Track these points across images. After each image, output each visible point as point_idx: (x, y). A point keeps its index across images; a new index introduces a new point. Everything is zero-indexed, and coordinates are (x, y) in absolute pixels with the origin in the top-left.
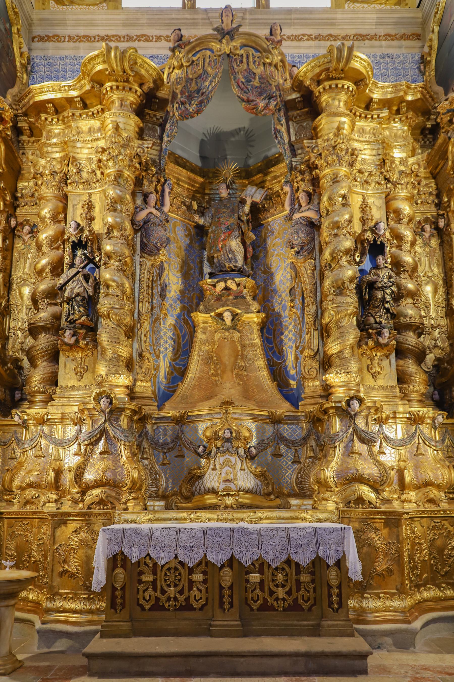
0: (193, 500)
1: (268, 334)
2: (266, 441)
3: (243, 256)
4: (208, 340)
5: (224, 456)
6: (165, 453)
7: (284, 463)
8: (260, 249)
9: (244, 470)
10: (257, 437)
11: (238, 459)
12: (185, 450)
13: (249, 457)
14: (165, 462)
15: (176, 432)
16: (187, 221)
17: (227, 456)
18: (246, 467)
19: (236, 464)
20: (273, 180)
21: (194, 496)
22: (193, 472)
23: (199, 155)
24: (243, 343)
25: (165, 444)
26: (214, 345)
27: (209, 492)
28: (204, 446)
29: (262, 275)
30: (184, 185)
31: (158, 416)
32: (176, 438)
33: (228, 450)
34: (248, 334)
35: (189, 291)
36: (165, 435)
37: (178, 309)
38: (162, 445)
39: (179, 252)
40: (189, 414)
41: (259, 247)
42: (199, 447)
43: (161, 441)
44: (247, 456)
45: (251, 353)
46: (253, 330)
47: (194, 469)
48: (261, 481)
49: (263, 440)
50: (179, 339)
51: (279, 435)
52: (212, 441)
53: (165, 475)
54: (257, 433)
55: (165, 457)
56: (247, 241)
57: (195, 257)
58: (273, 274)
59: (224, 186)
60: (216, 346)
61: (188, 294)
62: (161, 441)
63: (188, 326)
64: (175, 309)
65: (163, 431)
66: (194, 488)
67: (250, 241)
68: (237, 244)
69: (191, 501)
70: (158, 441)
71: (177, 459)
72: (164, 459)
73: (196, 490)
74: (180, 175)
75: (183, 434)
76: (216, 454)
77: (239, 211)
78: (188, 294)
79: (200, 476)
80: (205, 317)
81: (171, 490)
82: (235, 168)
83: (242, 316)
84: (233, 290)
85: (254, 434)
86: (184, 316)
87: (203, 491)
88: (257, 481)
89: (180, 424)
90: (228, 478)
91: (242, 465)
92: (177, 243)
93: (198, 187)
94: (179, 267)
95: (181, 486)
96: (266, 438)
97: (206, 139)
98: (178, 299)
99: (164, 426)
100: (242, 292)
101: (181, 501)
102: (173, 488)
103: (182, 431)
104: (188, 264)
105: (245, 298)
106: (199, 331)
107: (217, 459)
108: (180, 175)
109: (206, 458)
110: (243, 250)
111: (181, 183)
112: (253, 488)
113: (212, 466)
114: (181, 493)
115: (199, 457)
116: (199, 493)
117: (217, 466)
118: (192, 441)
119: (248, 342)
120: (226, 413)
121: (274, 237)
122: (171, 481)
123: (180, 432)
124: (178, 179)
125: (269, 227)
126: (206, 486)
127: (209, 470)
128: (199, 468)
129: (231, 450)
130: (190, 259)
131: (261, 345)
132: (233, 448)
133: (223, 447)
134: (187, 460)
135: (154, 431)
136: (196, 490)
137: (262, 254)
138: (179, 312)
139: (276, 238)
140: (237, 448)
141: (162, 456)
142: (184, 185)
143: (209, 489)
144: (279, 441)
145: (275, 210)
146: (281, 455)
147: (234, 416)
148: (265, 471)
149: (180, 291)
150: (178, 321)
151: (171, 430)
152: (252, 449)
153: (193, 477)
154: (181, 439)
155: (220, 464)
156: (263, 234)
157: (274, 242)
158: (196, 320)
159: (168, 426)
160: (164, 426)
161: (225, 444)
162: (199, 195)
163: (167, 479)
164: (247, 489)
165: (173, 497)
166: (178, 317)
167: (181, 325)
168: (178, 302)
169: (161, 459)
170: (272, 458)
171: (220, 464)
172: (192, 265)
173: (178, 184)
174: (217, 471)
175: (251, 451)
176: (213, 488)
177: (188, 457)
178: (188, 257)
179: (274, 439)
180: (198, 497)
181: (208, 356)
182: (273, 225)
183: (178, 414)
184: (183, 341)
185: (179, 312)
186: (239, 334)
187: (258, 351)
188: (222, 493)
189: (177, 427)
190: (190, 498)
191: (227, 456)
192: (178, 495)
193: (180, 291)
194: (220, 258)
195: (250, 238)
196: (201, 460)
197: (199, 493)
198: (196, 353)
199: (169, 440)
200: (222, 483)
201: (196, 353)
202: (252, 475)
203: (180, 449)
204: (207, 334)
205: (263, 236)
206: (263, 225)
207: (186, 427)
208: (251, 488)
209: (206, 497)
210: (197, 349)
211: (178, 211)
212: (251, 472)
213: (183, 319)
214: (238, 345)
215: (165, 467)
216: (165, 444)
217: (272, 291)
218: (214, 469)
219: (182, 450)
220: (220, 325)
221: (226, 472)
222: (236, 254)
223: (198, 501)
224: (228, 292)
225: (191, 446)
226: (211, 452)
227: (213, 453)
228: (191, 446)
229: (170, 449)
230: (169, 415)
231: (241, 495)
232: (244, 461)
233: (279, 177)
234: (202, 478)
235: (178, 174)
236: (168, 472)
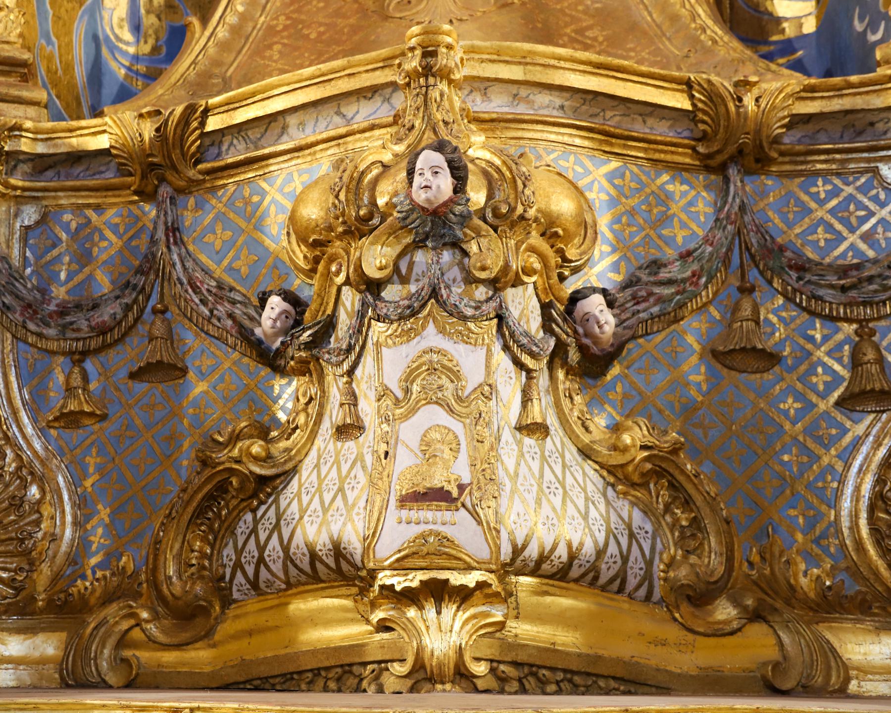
0: (226, 628)
2: (674, 271)
5: (408, 335)
6: (79, 357)
7: (791, 405)
9: (539, 430)
10: (620, 245)
11: (502, 360)
12: (190, 338)
13: (574, 356)
14: (72, 406)
15: (143, 243)
17: (431, 337)
18: (552, 421)
19: (488, 391)
21: (227, 601)
22: (222, 455)
25: (78, 307)
27: (315, 578)
28: (290, 297)
31: (40, 149)
32: (140, 271)
33: (434, 293)
36: (84, 258)
38: (63, 311)
40: (213, 123)
42: (263, 300)
43: (60, 293)
44: (560, 350)
47: (235, 438)
48: (647, 512)
49: (656, 265)
51: (754, 240)
52: (337, 247)
53: (75, 483)
54: (617, 220)
55: (76, 380)
62: (60, 293)
65: (74, 236)
66: (229, 551)
69: (209, 634)
70: (44, 291)
71: (140, 387)
72: (70, 390)
73: (238, 566)
75: (180, 243)
76: (360, 329)
79: (263, 480)
81: (100, 566)
85: (604, 223)
87: (277, 568)
88: (624, 507)
89: (165, 191)
90: (438, 481)
91: (526, 399)
95: (158, 542)
96: (670, 253)
99: (79, 209)
101: (151, 627)
102: (111, 556)
103: (174, 231)
107: (367, 364)
109: (303, 370)
112: (600, 553)
113: (335, 414)
114: (155, 584)
115: (265, 371)
116: (254, 584)
117: (367, 408)
118: (229, 280)
120: (427, 71)
122: (104, 512)
123: (160, 234)
126: (298, 539)
127: (319, 442)
128: (263, 433)
129: (456, 293)
132: (470, 280)
133: (404, 280)
134: (199, 388)
135: (24, 240)
136: (238, 566)
140: (496, 284)
141: (60, 378)
143: (314, 556)
144: (753, 275)
146: (770, 359)
147: (480, 105)
148: (675, 450)
151: (114, 228)
152: (595, 304)
153: (222, 488)
154: (166, 278)
155: (384, 393)
159: (98, 208)
160: (79, 209)
161: (420, 257)
163: (82, 503)
164: (562, 552)
165: (114, 607)
169: (55, 395)
170: (711, 375)
171: (384, 393)
174: (367, 438)
175: (586, 318)
176: (338, 551)
177: (202, 376)
179: (726, 261)
180: (253, 605)
183: (148, 130)
188: (399, 582)
189: (150, 210)
190: (205, 611)
191: (431, 337)
192: (137, 596)
196: (278, 383)
197: (254, 584)
199: (104, 283)
200: (393, 513)
202: (589, 467)
203: (159, 329)
207: (198, 207)
208: (589, 549)
209: (300, 606)
212: (586, 453)
215: (75, 436)
216: (78, 307)
218: (343, 431)
219: (170, 336)
221: (426, 444)
223: (250, 633)
225: (222, 310)
226: (330, 324)
227: (344, 321)
228: (222, 310)
229: (102, 330)
230: (102, 142)
231: (523, 596)
232: (543, 380)
234: (276, 492)
236: (92, 461)
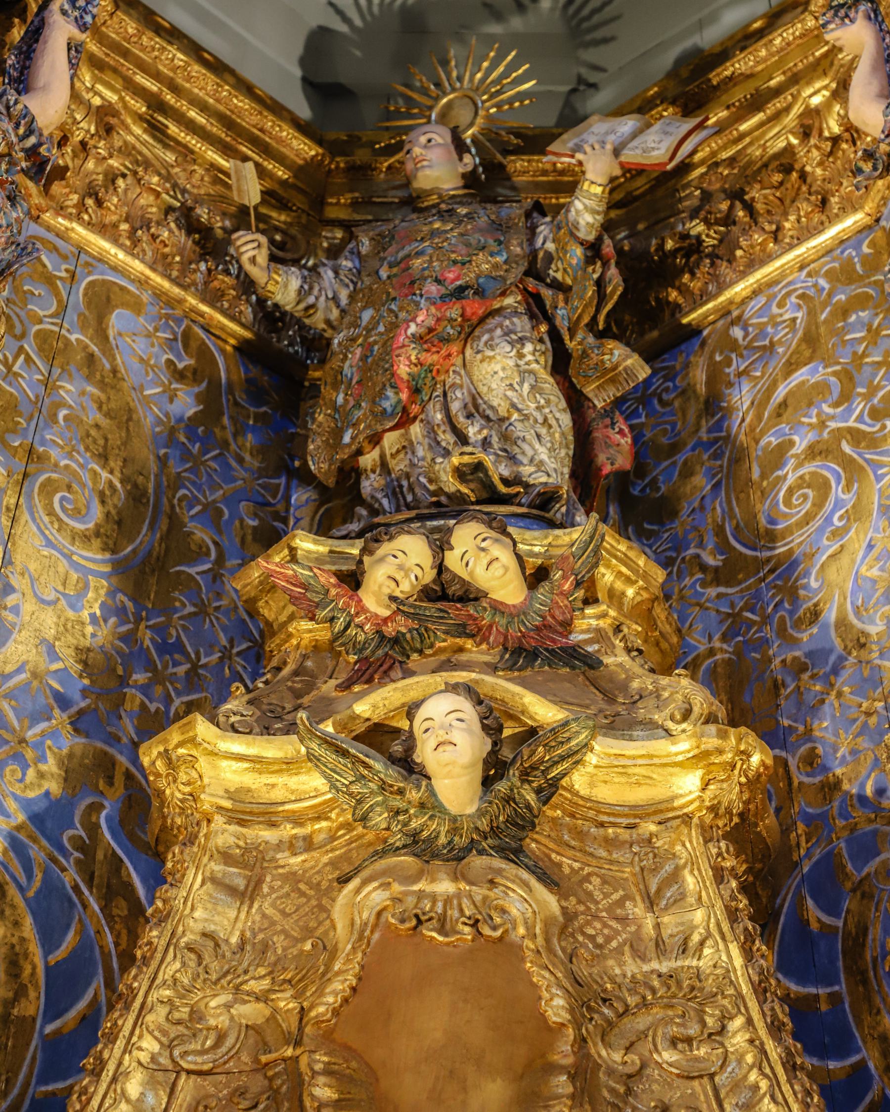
1: (801, 980)
3: (566, 453)
4: (265, 947)
8: (680, 458)
16: (192, 301)
20: (740, 117)
23: (297, 73)
24: (584, 971)
26: (325, 978)
29: (712, 592)
30: (192, 141)
34: (637, 909)
35: (158, 677)
37: (51, 765)
39: (115, 439)
41: (674, 448)
45: (668, 1056)
46: (675, 877)
50: (20, 992)
56: (589, 390)
57: (232, 500)
58: (794, 564)
59: (441, 136)
60: (339, 987)
61: (145, 689)
63: (121, 908)
64: (18, 757)
67: (613, 392)
68: (523, 374)
74: (175, 89)
77: (532, 232)
78: (145, 689)
80: (258, 763)
82: (505, 75)
83: (575, 756)
84: (497, 607)
86: (93, 829)
92: (102, 385)
93: (283, 183)
94: (97, 512)
97: (343, 28)
98: (63, 701)
100: (567, 626)
104: (175, 523)
105: (591, 663)
106: (193, 879)
108: (175, 89)
110: (566, 420)
111: (173, 129)
119: (632, 967)
121: (777, 364)
124: (157, 104)
125: (737, 333)
130: (192, 502)
131: (761, 991)
137: (700, 482)
138: (54, 787)
139: (791, 367)
142: (192, 141)
145: (776, 235)
149: (84, 655)
150: (37, 853)
156: (699, 376)
157: (781, 392)
158: (174, 793)
162: (283, 218)
166: (37, 819)
167: (50, 887)
168: (60, 717)
172: (201, 534)
173: (156, 130)
178: (178, 482)
181: (257, 1083)
184: (53, 1010)
185: (54, 787)
186: (551, 902)
187: (738, 1040)
193: (84, 655)
194: (399, 465)
195: (610, 375)
198: (150, 1044)
201: (150, 1044)
204: (265, 905)
205: (702, 389)
206: (694, 332)
210: (156, 1017)
211: (136, 242)
213: (80, 846)
214: (540, 978)
217: (798, 668)
220: (380, 819)
222: (519, 429)
224: (456, 612)
233: (777, 92)
235: (157, 76)
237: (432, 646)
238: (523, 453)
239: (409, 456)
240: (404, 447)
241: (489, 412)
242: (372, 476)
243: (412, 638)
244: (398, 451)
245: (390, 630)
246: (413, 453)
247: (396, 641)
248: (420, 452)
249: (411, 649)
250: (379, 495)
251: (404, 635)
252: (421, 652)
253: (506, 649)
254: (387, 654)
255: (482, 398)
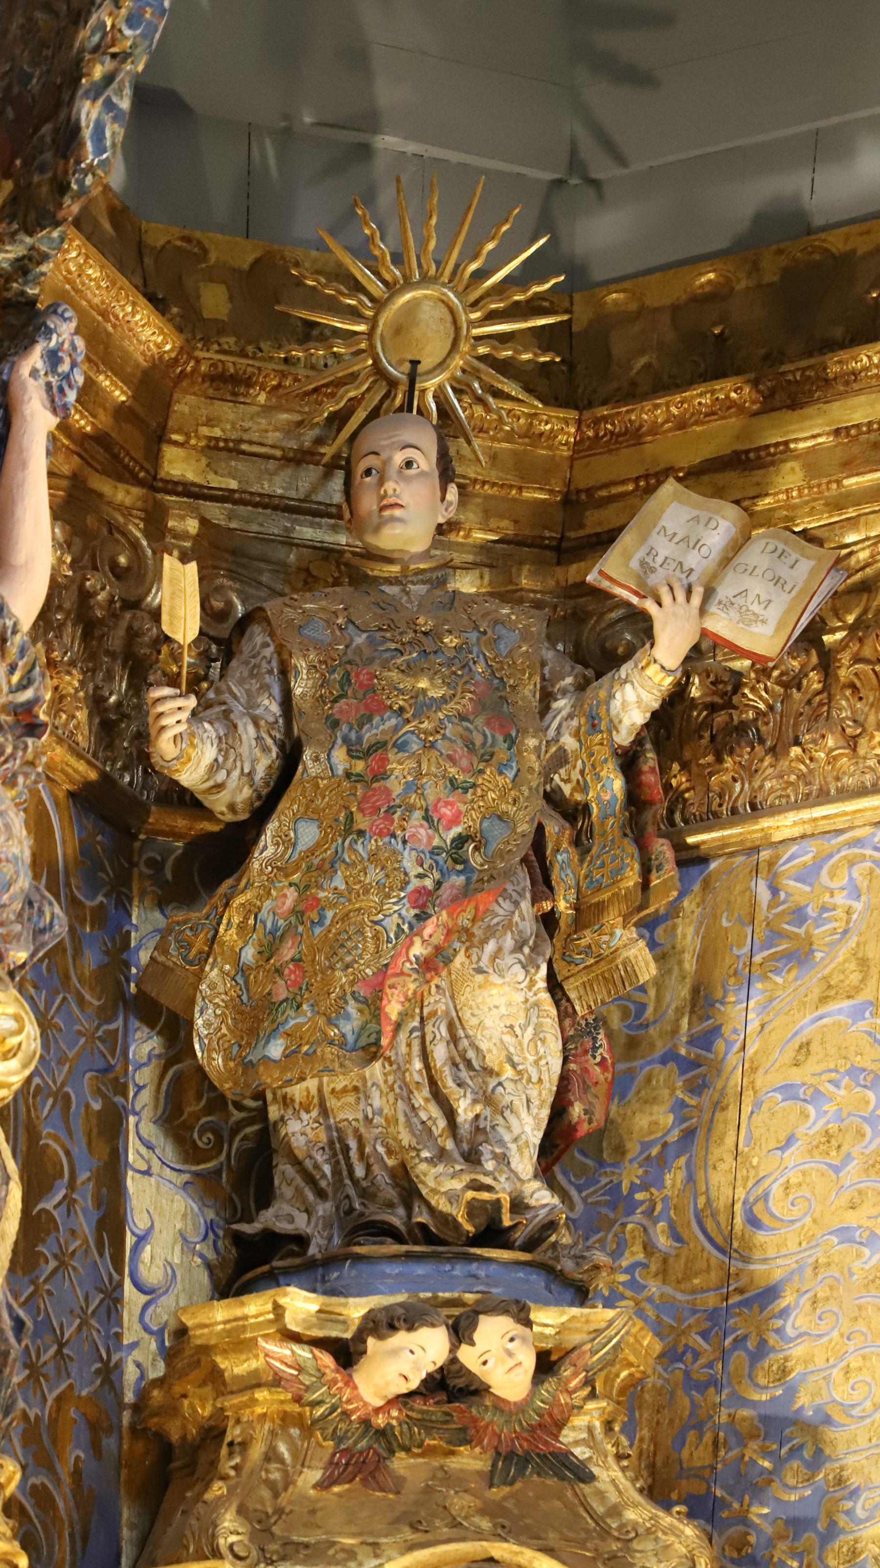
182: (809, 874)
237: (420, 1446)
238: (509, 1128)
239: (362, 1105)
240: (356, 1089)
241: (471, 1054)
242: (304, 1116)
243: (401, 1433)
244: (345, 1090)
245: (380, 1421)
246: (367, 1097)
247: (383, 1433)
248: (377, 1102)
249: (399, 1445)
250: (319, 1158)
251: (392, 1427)
252: (407, 1450)
253: (498, 1454)
254: (370, 1448)
255: (464, 1029)
